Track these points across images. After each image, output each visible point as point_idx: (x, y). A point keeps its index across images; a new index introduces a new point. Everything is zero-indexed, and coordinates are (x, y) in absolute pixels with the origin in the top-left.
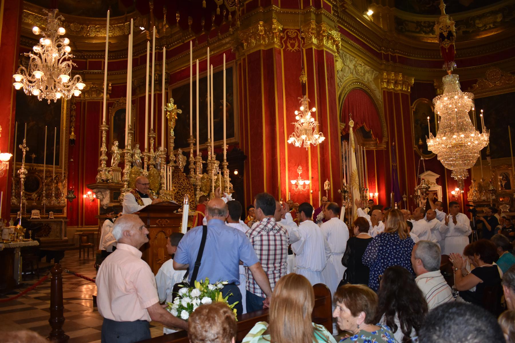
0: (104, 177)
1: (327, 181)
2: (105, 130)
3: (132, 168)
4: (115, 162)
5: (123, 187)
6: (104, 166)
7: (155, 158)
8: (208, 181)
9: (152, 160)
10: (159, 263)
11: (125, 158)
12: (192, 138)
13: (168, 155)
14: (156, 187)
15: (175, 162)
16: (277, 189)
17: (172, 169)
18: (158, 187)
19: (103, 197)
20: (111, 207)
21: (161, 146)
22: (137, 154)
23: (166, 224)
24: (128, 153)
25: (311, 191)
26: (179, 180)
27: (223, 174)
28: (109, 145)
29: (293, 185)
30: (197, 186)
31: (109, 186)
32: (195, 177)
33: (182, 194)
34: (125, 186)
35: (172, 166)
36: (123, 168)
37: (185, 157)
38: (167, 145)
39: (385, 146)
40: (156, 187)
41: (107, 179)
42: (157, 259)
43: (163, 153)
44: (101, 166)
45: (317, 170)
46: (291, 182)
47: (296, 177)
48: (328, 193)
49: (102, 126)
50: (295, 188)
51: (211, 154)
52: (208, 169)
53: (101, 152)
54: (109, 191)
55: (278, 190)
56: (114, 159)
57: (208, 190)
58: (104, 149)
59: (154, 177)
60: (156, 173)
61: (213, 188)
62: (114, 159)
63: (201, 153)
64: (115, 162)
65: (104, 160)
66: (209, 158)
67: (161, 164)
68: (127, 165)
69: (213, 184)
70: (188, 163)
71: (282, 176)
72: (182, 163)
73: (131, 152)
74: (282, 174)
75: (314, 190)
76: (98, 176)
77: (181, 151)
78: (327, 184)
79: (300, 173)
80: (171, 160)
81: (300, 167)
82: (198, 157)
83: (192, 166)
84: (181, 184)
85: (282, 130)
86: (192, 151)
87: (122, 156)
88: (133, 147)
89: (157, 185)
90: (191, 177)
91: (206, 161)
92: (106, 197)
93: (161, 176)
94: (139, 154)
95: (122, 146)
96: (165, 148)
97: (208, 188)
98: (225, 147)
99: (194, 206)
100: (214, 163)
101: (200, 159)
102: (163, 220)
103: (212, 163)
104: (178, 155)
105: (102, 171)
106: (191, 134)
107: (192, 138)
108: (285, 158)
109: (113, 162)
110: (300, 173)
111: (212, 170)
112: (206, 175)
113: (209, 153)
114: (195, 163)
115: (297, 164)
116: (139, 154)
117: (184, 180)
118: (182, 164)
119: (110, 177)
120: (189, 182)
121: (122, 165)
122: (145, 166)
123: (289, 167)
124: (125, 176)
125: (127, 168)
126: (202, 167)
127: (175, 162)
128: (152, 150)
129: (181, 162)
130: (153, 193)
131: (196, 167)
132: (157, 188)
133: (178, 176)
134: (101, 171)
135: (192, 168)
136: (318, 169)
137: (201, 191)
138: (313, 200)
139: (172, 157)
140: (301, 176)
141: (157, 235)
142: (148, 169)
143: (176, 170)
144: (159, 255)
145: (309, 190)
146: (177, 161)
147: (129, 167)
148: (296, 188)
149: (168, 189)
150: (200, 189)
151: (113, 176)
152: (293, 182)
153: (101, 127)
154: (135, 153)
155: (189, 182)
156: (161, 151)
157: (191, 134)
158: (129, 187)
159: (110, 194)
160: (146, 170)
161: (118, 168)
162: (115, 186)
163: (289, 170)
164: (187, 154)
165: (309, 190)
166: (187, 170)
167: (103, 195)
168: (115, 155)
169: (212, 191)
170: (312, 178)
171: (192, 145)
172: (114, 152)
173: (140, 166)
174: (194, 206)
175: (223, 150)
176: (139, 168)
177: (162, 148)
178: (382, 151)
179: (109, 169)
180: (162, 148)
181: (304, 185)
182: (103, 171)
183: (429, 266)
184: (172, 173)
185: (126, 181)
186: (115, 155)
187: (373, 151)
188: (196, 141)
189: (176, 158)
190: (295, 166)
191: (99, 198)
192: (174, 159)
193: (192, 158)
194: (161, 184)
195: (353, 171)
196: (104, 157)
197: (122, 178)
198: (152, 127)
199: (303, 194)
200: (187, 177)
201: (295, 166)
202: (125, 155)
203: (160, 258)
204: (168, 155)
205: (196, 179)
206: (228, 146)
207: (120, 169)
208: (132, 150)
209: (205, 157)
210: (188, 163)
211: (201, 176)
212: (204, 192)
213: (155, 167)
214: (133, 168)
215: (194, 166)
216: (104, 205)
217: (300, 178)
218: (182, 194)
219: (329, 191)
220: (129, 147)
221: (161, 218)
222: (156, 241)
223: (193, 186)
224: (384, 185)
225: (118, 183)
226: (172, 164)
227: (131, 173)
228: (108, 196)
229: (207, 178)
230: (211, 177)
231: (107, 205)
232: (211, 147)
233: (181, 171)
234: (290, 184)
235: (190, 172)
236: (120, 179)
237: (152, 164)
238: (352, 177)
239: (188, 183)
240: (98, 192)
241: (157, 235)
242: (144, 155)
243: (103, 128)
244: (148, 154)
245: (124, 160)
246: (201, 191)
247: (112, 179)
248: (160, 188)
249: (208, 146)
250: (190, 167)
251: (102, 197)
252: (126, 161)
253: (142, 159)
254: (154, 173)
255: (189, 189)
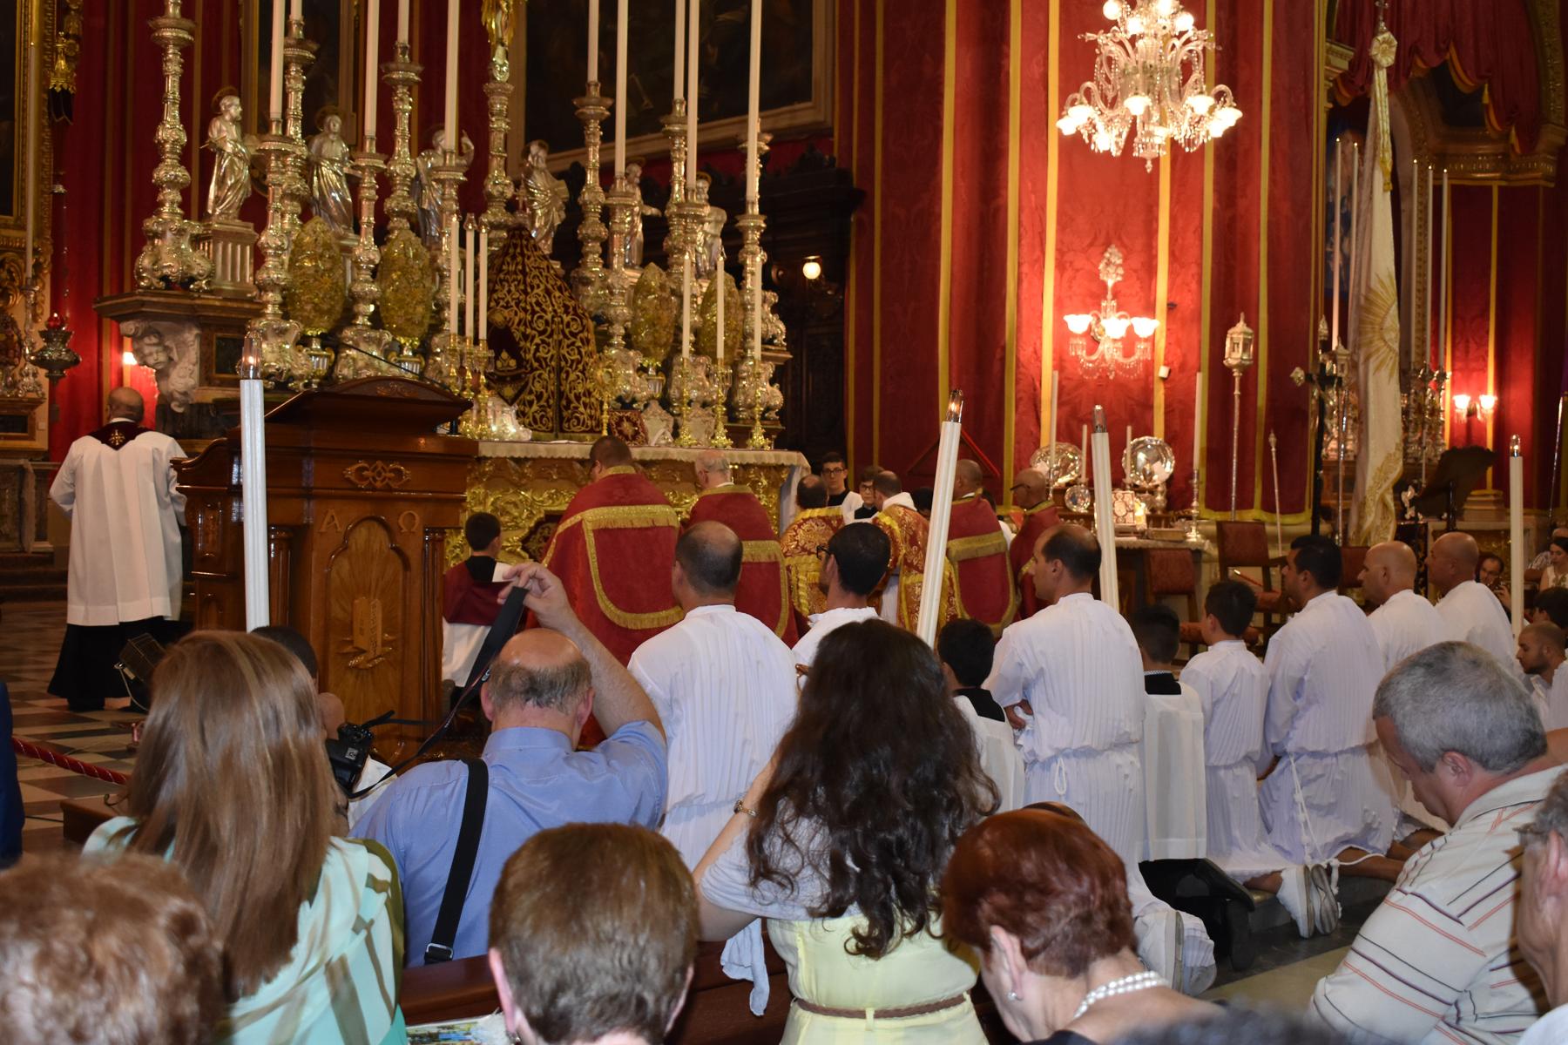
0: (171, 265)
1: (1241, 326)
2: (178, 42)
3: (301, 226)
4: (223, 196)
5: (259, 314)
6: (173, 213)
7: (416, 186)
8: (668, 300)
9: (401, 191)
10: (356, 667)
11: (270, 177)
12: (595, 92)
13: (477, 170)
14: (417, 319)
15: (512, 206)
16: (999, 350)
17: (490, 243)
18: (427, 321)
19: (171, 359)
20: (207, 405)
21: (443, 128)
22: (332, 162)
23: (394, 485)
24: (282, 155)
25: (1163, 372)
26: (526, 293)
27: (736, 270)
28: (199, 116)
29: (1075, 336)
30: (611, 324)
31: (192, 307)
32: (604, 279)
33: (537, 360)
34: (270, 309)
35: (493, 227)
36: (261, 226)
37: (563, 187)
38: (474, 120)
39: (1551, 169)
40: (417, 319)
41: (184, 273)
42: (349, 649)
43: (452, 161)
44: (159, 214)
45: (1194, 269)
46: (1065, 323)
47: (1093, 299)
48: (1242, 380)
49: (162, 21)
50: (1082, 353)
51: (685, 171)
52: (667, 243)
53: (161, 144)
54: (196, 331)
55: (1003, 359)
56: (221, 182)
57: (665, 345)
58: (171, 131)
59: (405, 271)
60: (416, 256)
61: (687, 338)
62: (221, 182)
63: (637, 170)
64: (223, 196)
65: (172, 184)
66: (678, 193)
67: (442, 210)
68: (276, 210)
69: (688, 319)
70: (575, 212)
71: (1023, 297)
72: (546, 215)
73: (302, 151)
74: (1025, 285)
75: (1176, 365)
76: (145, 261)
77: (542, 154)
78: (1240, 338)
79: (1110, 283)
80: (490, 196)
81: (1114, 255)
82: (621, 186)
83: (592, 227)
84: (534, 312)
85: (1037, 71)
86: (594, 157)
87: (258, 165)
88: (311, 128)
89: (420, 309)
90: (587, 282)
91: (662, 207)
92: (182, 355)
93: (439, 270)
94: (342, 162)
95: (256, 122)
96: (466, 140)
97: (665, 336)
98: (755, 144)
99: (591, 417)
100: (700, 220)
101: (627, 194)
102: (379, 463)
103: (685, 217)
104: (529, 175)
105: (161, 236)
106: (593, 74)
107: (595, 92)
108: (1042, 208)
109: (217, 197)
110: (1110, 283)
111: (682, 252)
112: (654, 274)
113: (678, 169)
114: (607, 215)
115: (1101, 240)
116: (342, 162)
117: (548, 292)
118: (543, 218)
119: (199, 263)
120: (571, 304)
121: (255, 210)
122: (365, 219)
123: (1060, 252)
124: (270, 263)
125: (279, 228)
126: (640, 236)
127: (512, 206)
128: (402, 148)
129: (543, 206)
130: (401, 347)
131: (611, 234)
132: (421, 323)
133: (523, 272)
134: (156, 235)
135: (596, 239)
136: (1200, 265)
137: (629, 345)
138: (1166, 413)
139: (498, 182)
140: (1115, 296)
141: (347, 535)
142: (381, 236)
143: (516, 240)
144: (356, 626)
145: (1149, 367)
146: (522, 198)
147: (293, 223)
148: (1091, 352)
149: (469, 332)
150: (627, 337)
151: (214, 261)
152: (1078, 323)
153: (159, 28)
154: (320, 156)
155: (571, 304)
156: (445, 153)
157: (593, 74)
158: (286, 317)
159: (201, 345)
160: (367, 239)
161: (238, 226)
162: (222, 308)
163: (1060, 266)
164: (574, 178)
165: (1149, 367)
166: (568, 246)
167: (167, 349)
168: (226, 163)
169: (680, 351)
170: (1171, 307)
171: (594, 127)
172: (221, 151)
173: (345, 221)
174: (591, 417)
175: (743, 157)
176: (341, 230)
177: (449, 136)
178: (1537, 187)
179: (197, 228)
180: (449, 136)
181: (1130, 340)
182: (169, 235)
183: (1501, 742)
184: (492, 257)
185: (274, 286)
186: (226, 163)
187: (1490, 189)
188: (612, 109)
189: (517, 185)
190: (1091, 245)
191: (151, 361)
192: (509, 193)
193: (591, 190)
194: (442, 306)
195: (1374, 284)
196: (169, 171)
197: (254, 274)
198: (403, 35)
199: (1119, 385)
200: (566, 278)
201: (1091, 245)
202: (269, 161)
203: (361, 642)
204: (477, 170)
205: (610, 287)
206: (768, 138)
207: (249, 228)
208: (308, 144)
209: (656, 184)
210: (575, 212)
211: (633, 276)
212: (646, 353)
213: (415, 228)
214: (308, 227)
215: (604, 233)
216: (171, 397)
217: (1109, 303)
218: (537, 360)
219: (1249, 372)
220: (294, 129)
221: (371, 457)
222: (344, 565)
223: (591, 324)
224: (1529, 357)
225: (239, 296)
226: (495, 214)
227: (298, 249)
228: (193, 353)
229: (662, 287)
230: (680, 283)
231: (185, 394)
232: (686, 140)
233: (536, 248)
234: (1062, 334)
235: (582, 256)
236: (249, 279)
237: (403, 214)
238: (1368, 311)
239: (566, 307)
240: (147, 333)
241: (347, 535)
242: (363, 169)
243: (168, 34)
244: (380, 164)
245: (265, 189)
246: (629, 345)
247: (211, 275)
248: (437, 326)
249: (674, 135)
250: (583, 231)
251: (162, 358)
252: (275, 194)
253: (354, 184)
254: (406, 254)
255: (574, 335)
